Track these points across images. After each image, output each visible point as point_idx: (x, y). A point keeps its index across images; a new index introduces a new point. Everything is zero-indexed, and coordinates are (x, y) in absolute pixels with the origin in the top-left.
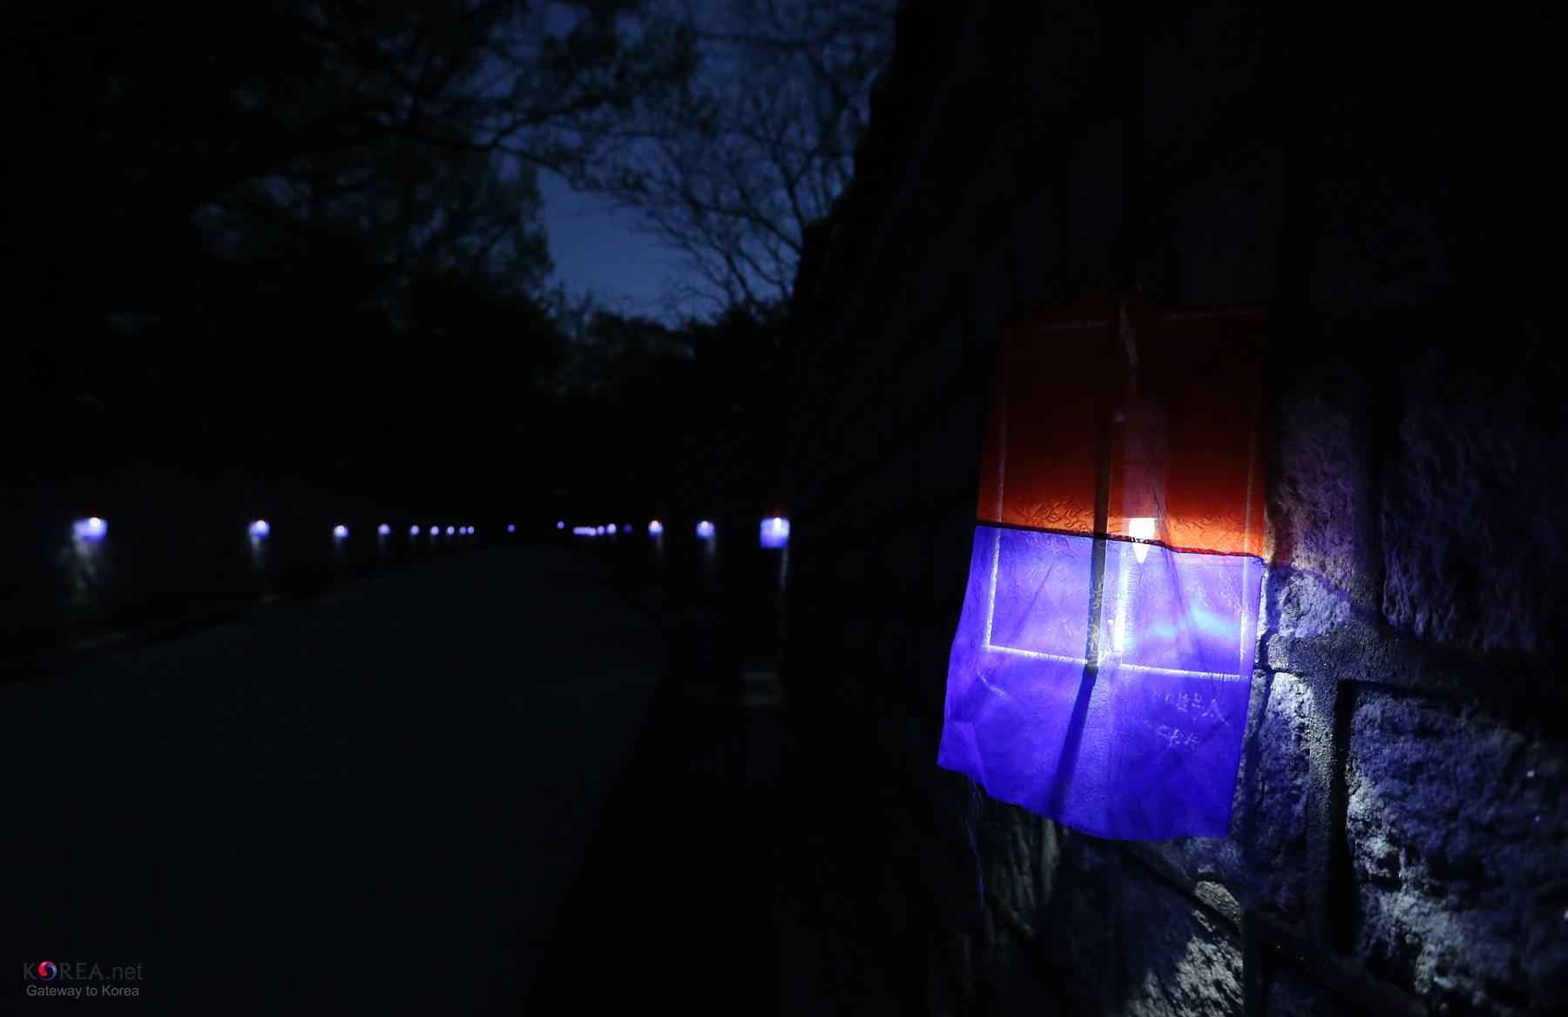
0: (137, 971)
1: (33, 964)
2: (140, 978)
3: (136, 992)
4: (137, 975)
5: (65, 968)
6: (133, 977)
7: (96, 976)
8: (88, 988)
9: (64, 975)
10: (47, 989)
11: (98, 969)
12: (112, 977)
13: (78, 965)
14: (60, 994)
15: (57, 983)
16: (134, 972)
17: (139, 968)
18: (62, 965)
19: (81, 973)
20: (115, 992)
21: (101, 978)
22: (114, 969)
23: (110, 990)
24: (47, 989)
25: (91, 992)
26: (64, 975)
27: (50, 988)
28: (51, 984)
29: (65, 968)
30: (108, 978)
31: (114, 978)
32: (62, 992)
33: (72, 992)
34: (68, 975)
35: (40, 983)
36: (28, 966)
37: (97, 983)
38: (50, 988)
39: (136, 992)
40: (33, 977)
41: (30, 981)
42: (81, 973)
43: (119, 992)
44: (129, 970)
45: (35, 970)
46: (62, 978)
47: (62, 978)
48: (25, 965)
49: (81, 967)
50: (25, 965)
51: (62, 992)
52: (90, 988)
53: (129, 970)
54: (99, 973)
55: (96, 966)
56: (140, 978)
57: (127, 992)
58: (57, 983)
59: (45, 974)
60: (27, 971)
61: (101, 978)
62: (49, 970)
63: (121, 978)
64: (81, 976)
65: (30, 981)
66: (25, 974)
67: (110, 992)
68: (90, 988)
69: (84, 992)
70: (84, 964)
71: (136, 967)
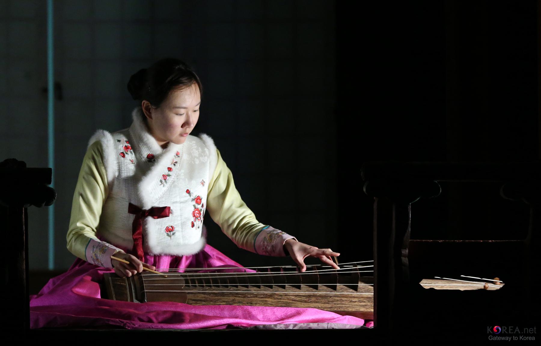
0: (534, 330)
1: (491, 327)
2: (535, 333)
3: (534, 338)
4: (534, 331)
5: (504, 328)
6: (533, 332)
7: (517, 332)
8: (514, 337)
9: (504, 331)
10: (497, 337)
11: (518, 329)
12: (523, 332)
13: (510, 327)
14: (502, 339)
15: (501, 335)
16: (533, 331)
17: (535, 328)
18: (503, 327)
19: (511, 330)
20: (525, 338)
21: (519, 333)
22: (525, 329)
23: (523, 338)
24: (497, 337)
25: (515, 338)
26: (504, 331)
27: (498, 337)
28: (499, 335)
29: (504, 328)
30: (522, 333)
31: (525, 333)
32: (503, 338)
33: (507, 338)
34: (505, 331)
35: (494, 335)
36: (489, 328)
37: (517, 335)
38: (498, 337)
39: (534, 338)
40: (492, 333)
41: (490, 334)
42: (511, 330)
43: (527, 338)
44: (531, 330)
45: (492, 330)
46: (503, 333)
47: (503, 333)
48: (488, 327)
49: (511, 328)
50: (488, 327)
51: (503, 338)
52: (515, 337)
53: (531, 330)
54: (518, 330)
55: (517, 328)
56: (535, 333)
57: (530, 338)
58: (501, 335)
59: (496, 331)
60: (489, 330)
61: (519, 333)
62: (498, 330)
63: (528, 333)
64: (511, 332)
65: (490, 334)
66: (520, 338)
67: (523, 339)
68: (515, 337)
69: (512, 339)
70: (512, 327)
71: (533, 328)
